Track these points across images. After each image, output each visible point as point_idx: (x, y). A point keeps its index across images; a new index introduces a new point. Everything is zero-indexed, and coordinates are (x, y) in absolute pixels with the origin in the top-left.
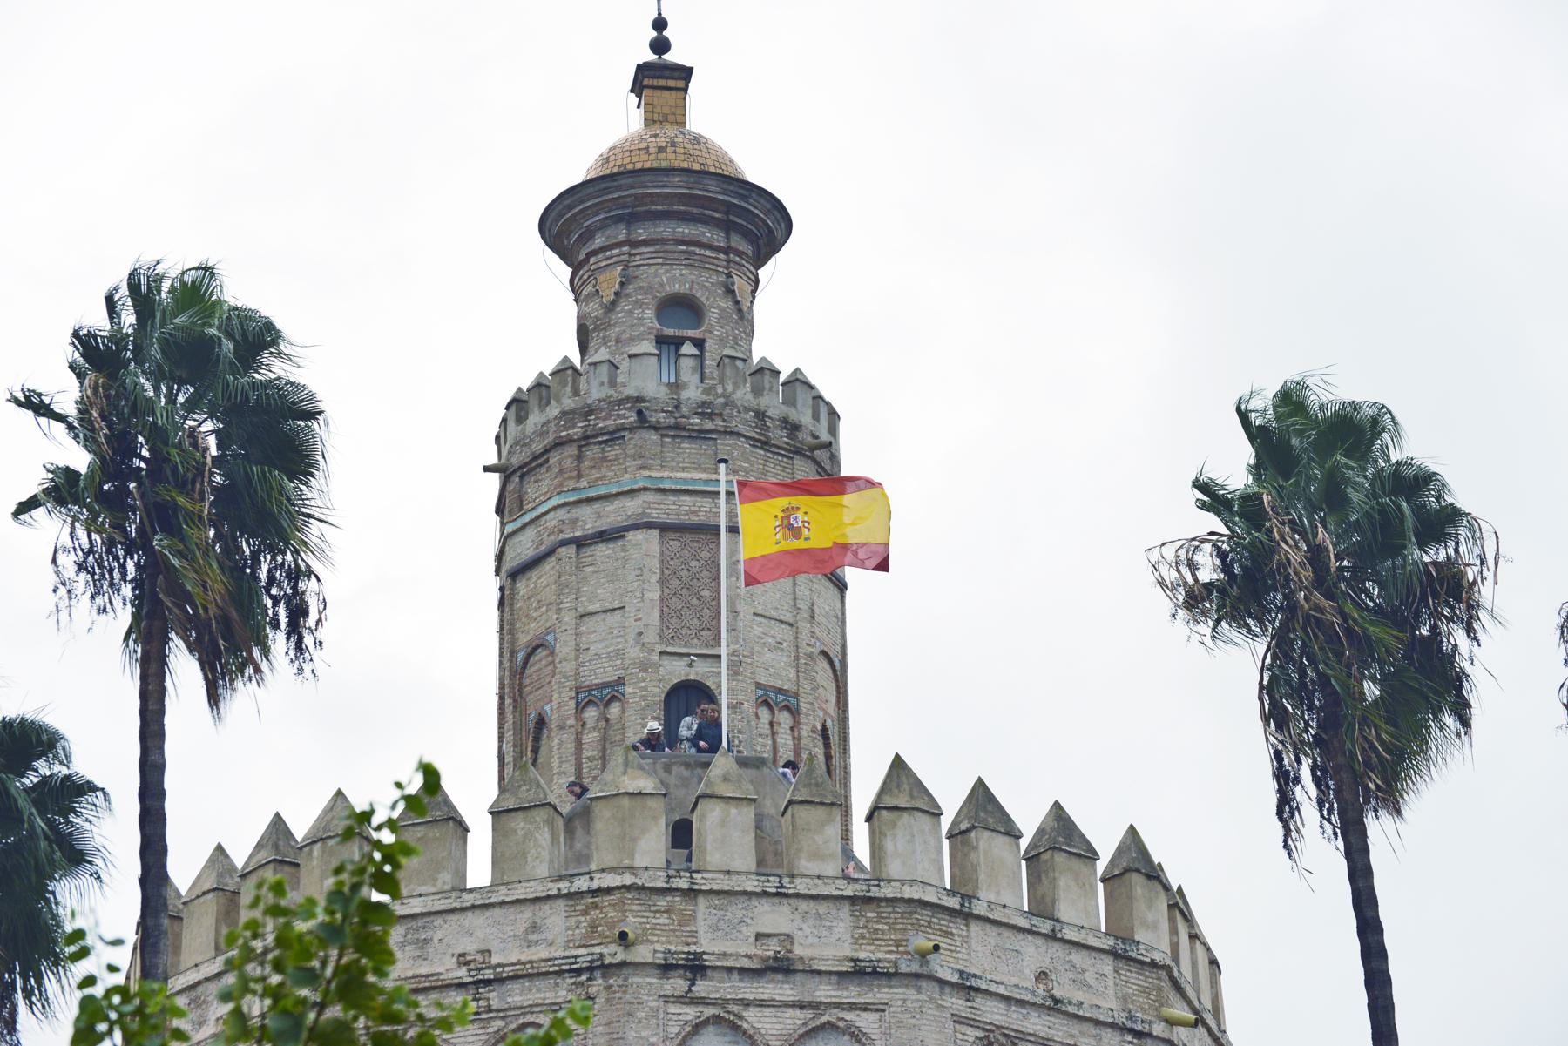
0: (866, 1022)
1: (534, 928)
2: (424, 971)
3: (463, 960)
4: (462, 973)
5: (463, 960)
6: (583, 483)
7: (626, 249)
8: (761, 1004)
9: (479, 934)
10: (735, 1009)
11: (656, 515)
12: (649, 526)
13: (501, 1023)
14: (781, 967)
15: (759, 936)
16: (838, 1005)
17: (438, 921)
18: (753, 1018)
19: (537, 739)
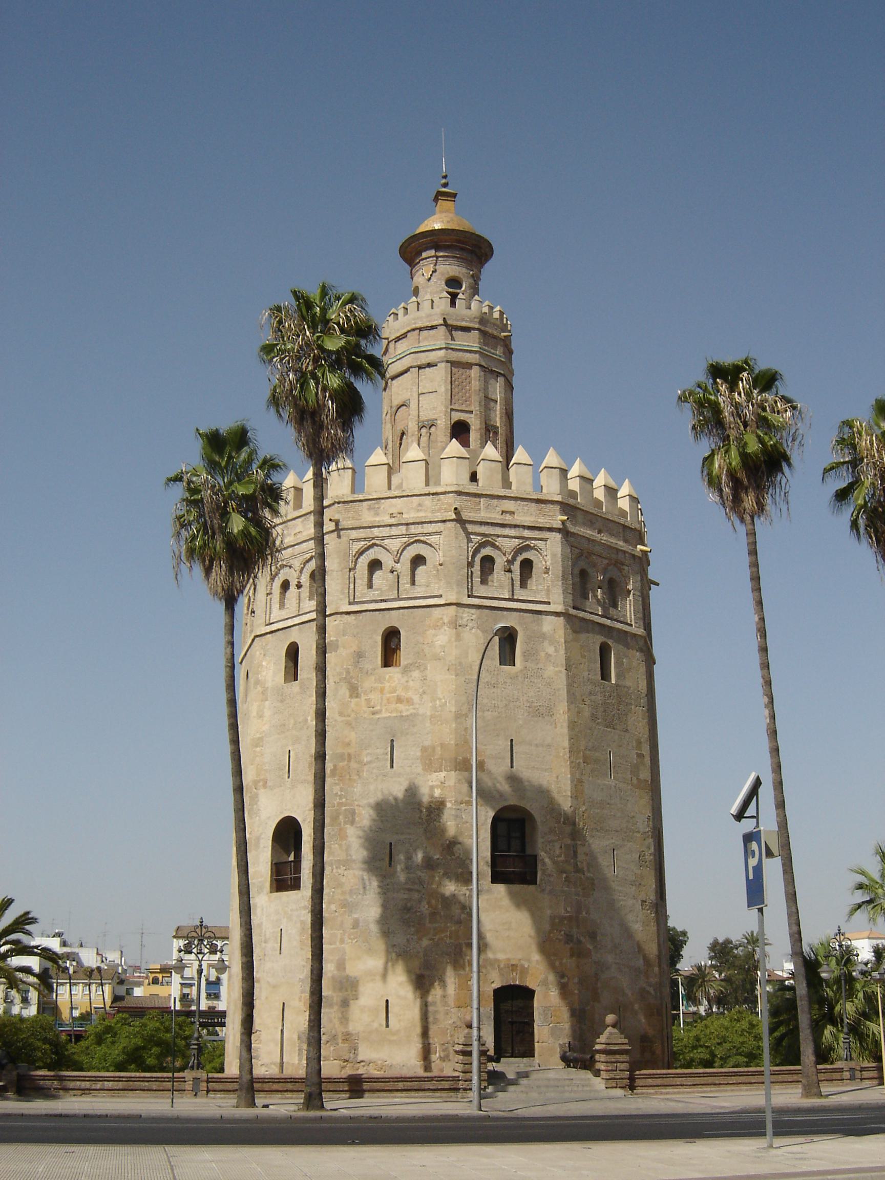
0: (540, 544)
1: (420, 505)
2: (377, 519)
6: (421, 344)
8: (504, 536)
12: (447, 362)
15: (503, 512)
17: (383, 501)
18: (499, 541)
19: (401, 439)
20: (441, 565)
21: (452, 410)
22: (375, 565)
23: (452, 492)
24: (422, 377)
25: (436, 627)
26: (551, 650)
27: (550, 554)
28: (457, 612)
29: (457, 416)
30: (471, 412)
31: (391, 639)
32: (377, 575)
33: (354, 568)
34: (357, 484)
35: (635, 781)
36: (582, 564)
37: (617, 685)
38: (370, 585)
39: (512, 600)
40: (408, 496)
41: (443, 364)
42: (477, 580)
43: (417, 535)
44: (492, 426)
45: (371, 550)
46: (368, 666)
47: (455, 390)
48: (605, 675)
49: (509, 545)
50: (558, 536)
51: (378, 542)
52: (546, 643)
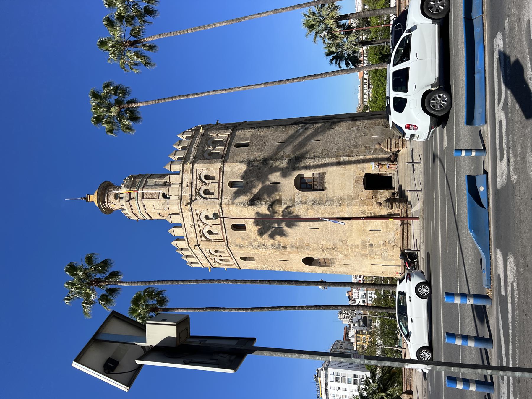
0: (198, 172)
3: (191, 227)
4: (193, 227)
5: (191, 227)
8: (196, 186)
14: (192, 184)
18: (198, 188)
22: (210, 232)
25: (230, 212)
26: (237, 168)
27: (202, 168)
29: (161, 197)
31: (236, 227)
32: (213, 231)
34: (181, 239)
35: (285, 132)
36: (206, 155)
37: (250, 140)
38: (217, 234)
39: (219, 183)
42: (212, 196)
46: (245, 236)
47: (152, 197)
48: (246, 145)
49: (199, 184)
50: (195, 165)
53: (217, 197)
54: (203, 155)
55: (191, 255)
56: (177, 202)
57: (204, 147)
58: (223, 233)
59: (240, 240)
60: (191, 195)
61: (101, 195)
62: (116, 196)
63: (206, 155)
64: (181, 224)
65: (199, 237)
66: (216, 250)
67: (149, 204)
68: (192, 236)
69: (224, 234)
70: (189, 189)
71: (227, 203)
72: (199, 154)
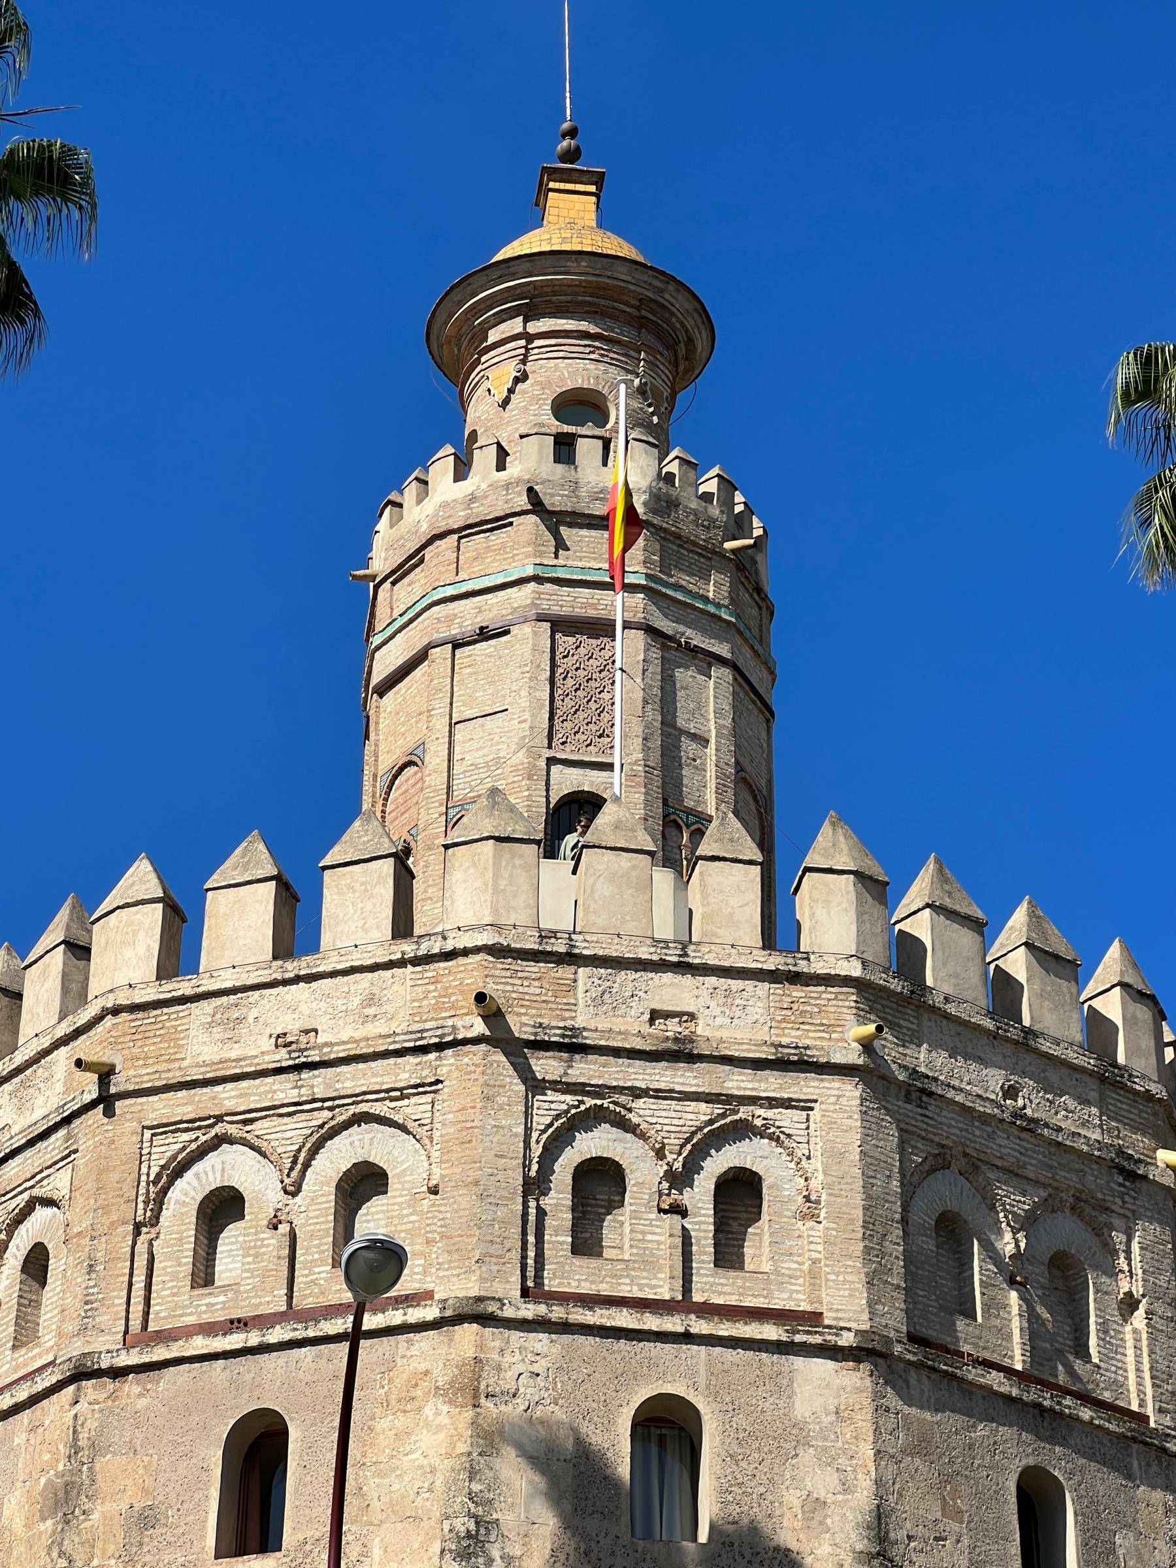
0: (787, 1119)
1: (371, 1000)
3: (281, 1041)
4: (282, 1057)
7: (523, 342)
8: (659, 1094)
9: (304, 1008)
10: (622, 1099)
11: (546, 606)
12: (540, 618)
13: (327, 1114)
15: (655, 1015)
16: (753, 1100)
18: (642, 1111)
20: (434, 1191)
21: (551, 761)
22: (222, 1208)
23: (477, 950)
24: (462, 673)
26: (822, 1483)
28: (481, 1347)
29: (567, 781)
30: (609, 767)
31: (257, 1455)
32: (231, 1238)
33: (155, 1220)
34: (179, 948)
38: (203, 1274)
39: (684, 1305)
40: (334, 974)
41: (527, 629)
42: (558, 1238)
43: (357, 1097)
44: (690, 812)
45: (212, 1158)
47: (565, 706)
50: (849, 1092)
51: (233, 1130)
52: (807, 1456)
53: (551, 1283)
54: (939, 1162)
55: (27, 1029)
56: (521, 917)
57: (1014, 1175)
58: (209, 1329)
59: (134, 1498)
60: (573, 1046)
61: (595, 290)
62: (578, 407)
63: (946, 1191)
64: (313, 946)
65: (181, 1106)
66: (55, 1266)
67: (510, 676)
68: (200, 1042)
69: (200, 1345)
70: (628, 1025)
71: (489, 1381)
72: (951, 1129)
